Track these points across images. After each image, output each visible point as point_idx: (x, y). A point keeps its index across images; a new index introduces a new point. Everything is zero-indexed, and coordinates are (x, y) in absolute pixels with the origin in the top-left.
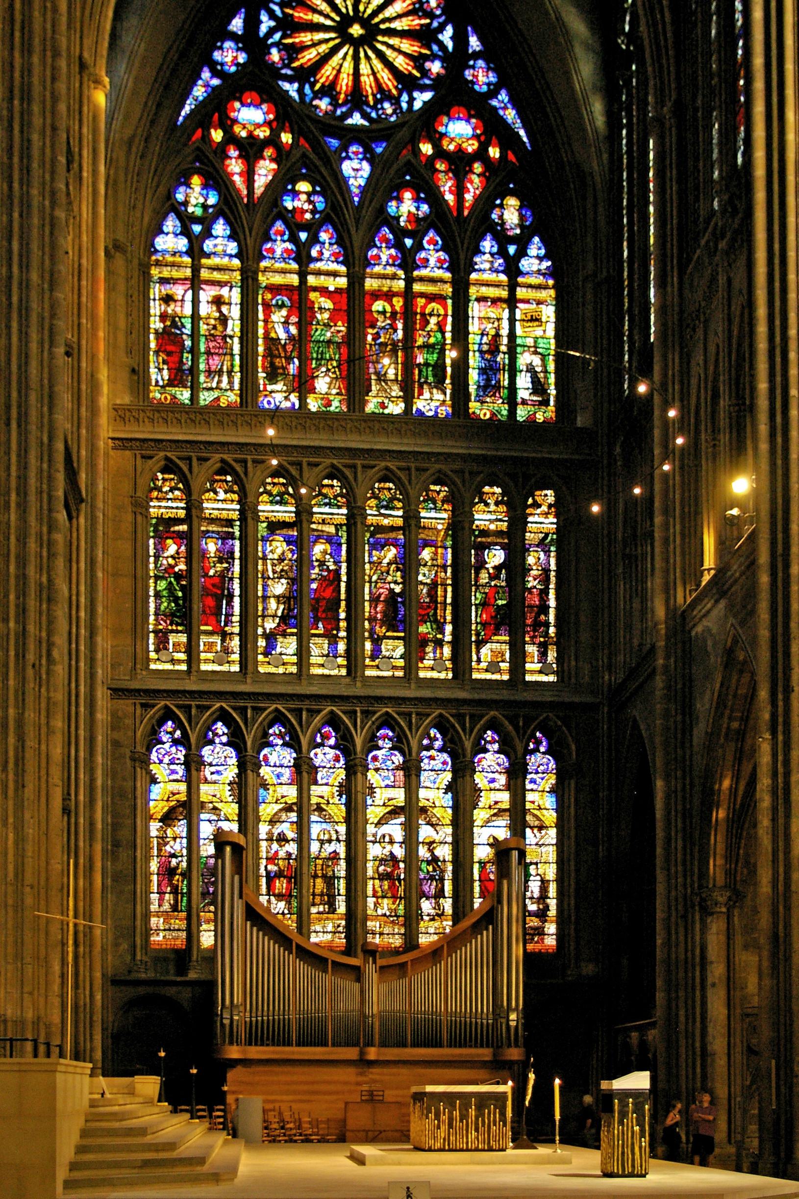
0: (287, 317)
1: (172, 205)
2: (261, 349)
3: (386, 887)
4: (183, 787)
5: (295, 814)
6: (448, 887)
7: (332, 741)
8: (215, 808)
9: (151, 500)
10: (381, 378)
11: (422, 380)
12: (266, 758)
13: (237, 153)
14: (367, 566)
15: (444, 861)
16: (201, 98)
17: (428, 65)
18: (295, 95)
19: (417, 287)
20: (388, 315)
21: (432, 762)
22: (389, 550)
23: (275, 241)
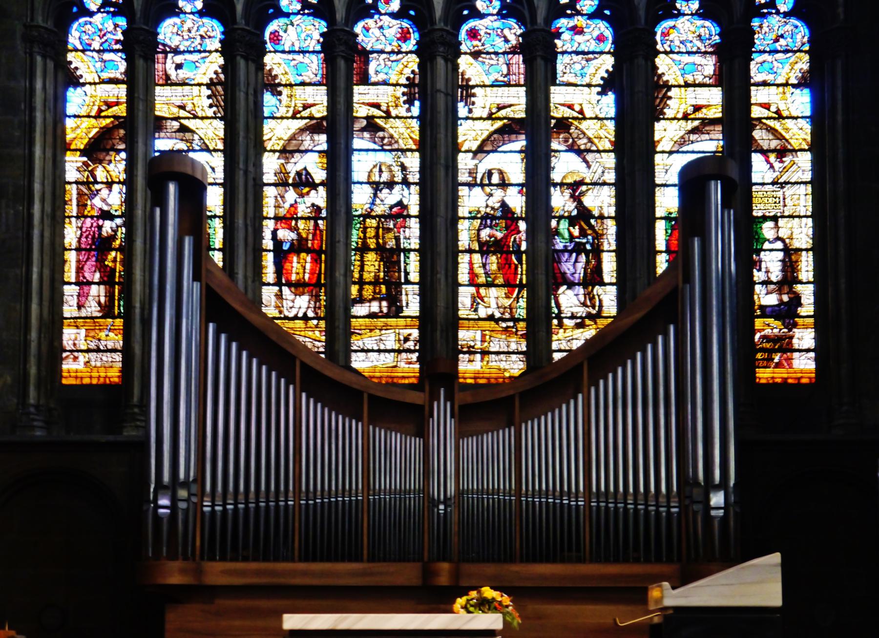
3: (494, 267)
4: (121, 91)
5: (323, 138)
6: (609, 264)
8: (183, 129)
12: (276, 38)
15: (602, 217)
21: (578, 38)
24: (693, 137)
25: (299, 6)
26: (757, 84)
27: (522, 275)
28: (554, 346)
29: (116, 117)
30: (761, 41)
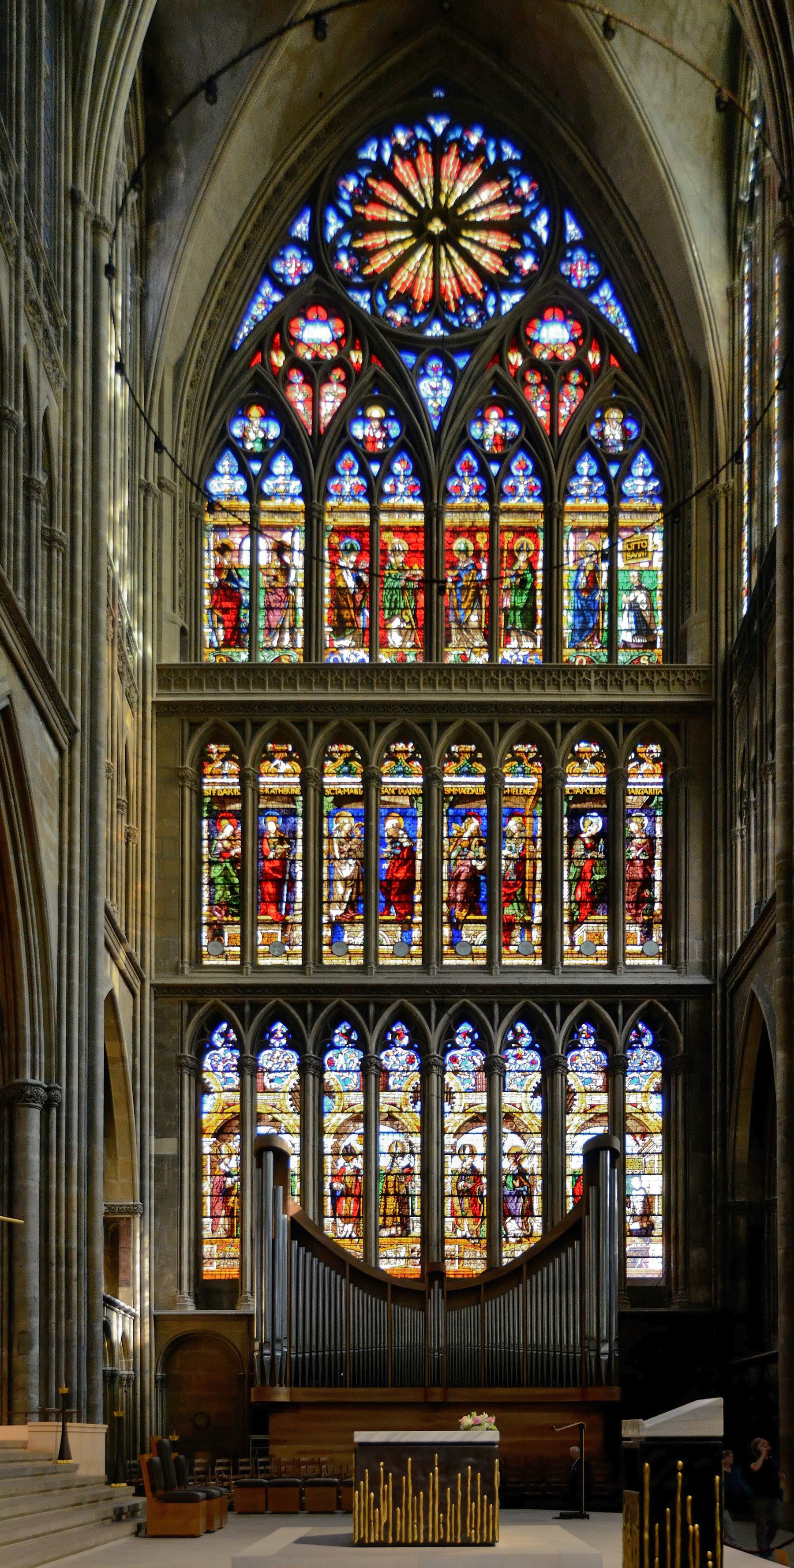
0: (357, 562)
1: (229, 441)
2: (327, 600)
3: (467, 1205)
4: (236, 1096)
6: (537, 1203)
7: (406, 1041)
8: (274, 1120)
9: (205, 776)
10: (463, 626)
11: (510, 626)
12: (331, 1062)
13: (301, 378)
14: (446, 841)
15: (533, 1174)
16: (261, 318)
18: (366, 306)
19: (504, 520)
20: (471, 554)
21: (519, 1062)
22: (472, 822)
23: (344, 476)
24: (589, 1124)
25: (345, 1042)
26: (630, 1092)
27: (484, 1211)
28: (504, 1254)
29: (233, 1113)
30: (633, 1064)
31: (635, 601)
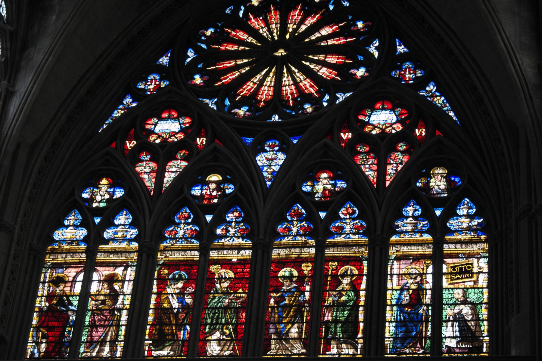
0: (184, 288)
2: (150, 318)
17: (353, 71)
19: (329, 252)
20: (295, 279)
23: (179, 224)
31: (460, 313)
